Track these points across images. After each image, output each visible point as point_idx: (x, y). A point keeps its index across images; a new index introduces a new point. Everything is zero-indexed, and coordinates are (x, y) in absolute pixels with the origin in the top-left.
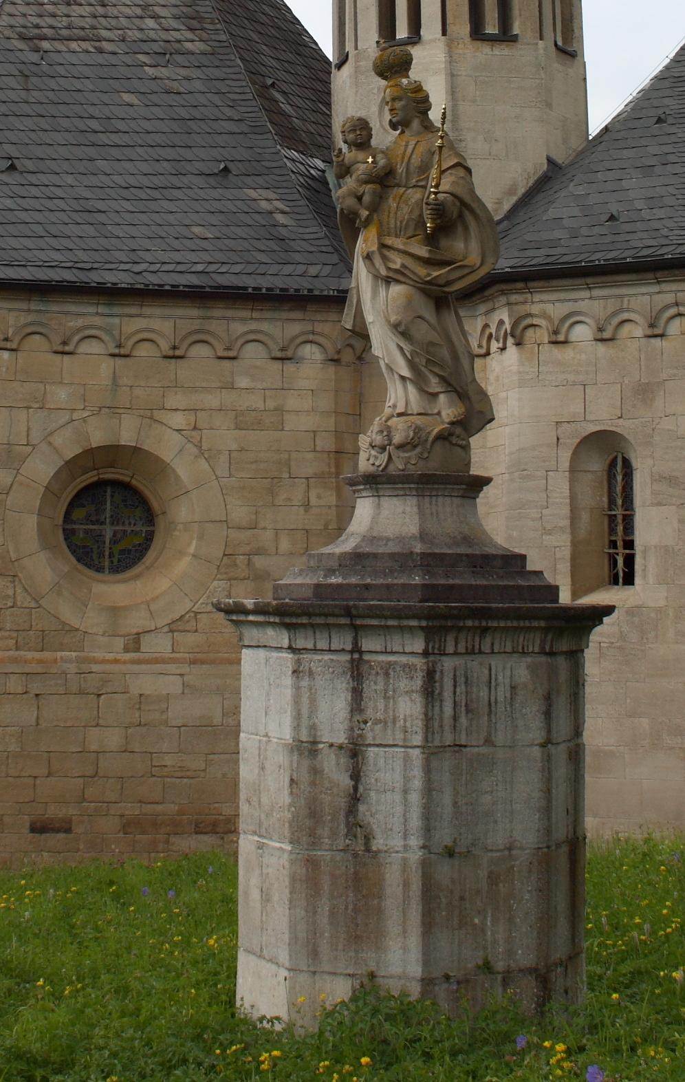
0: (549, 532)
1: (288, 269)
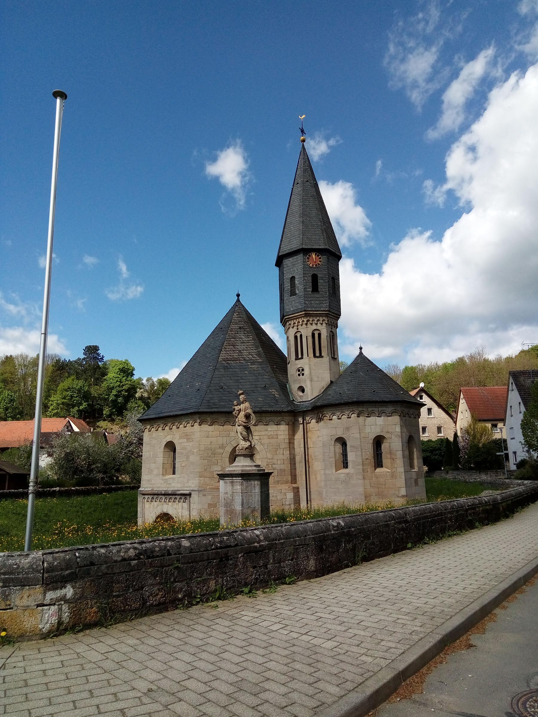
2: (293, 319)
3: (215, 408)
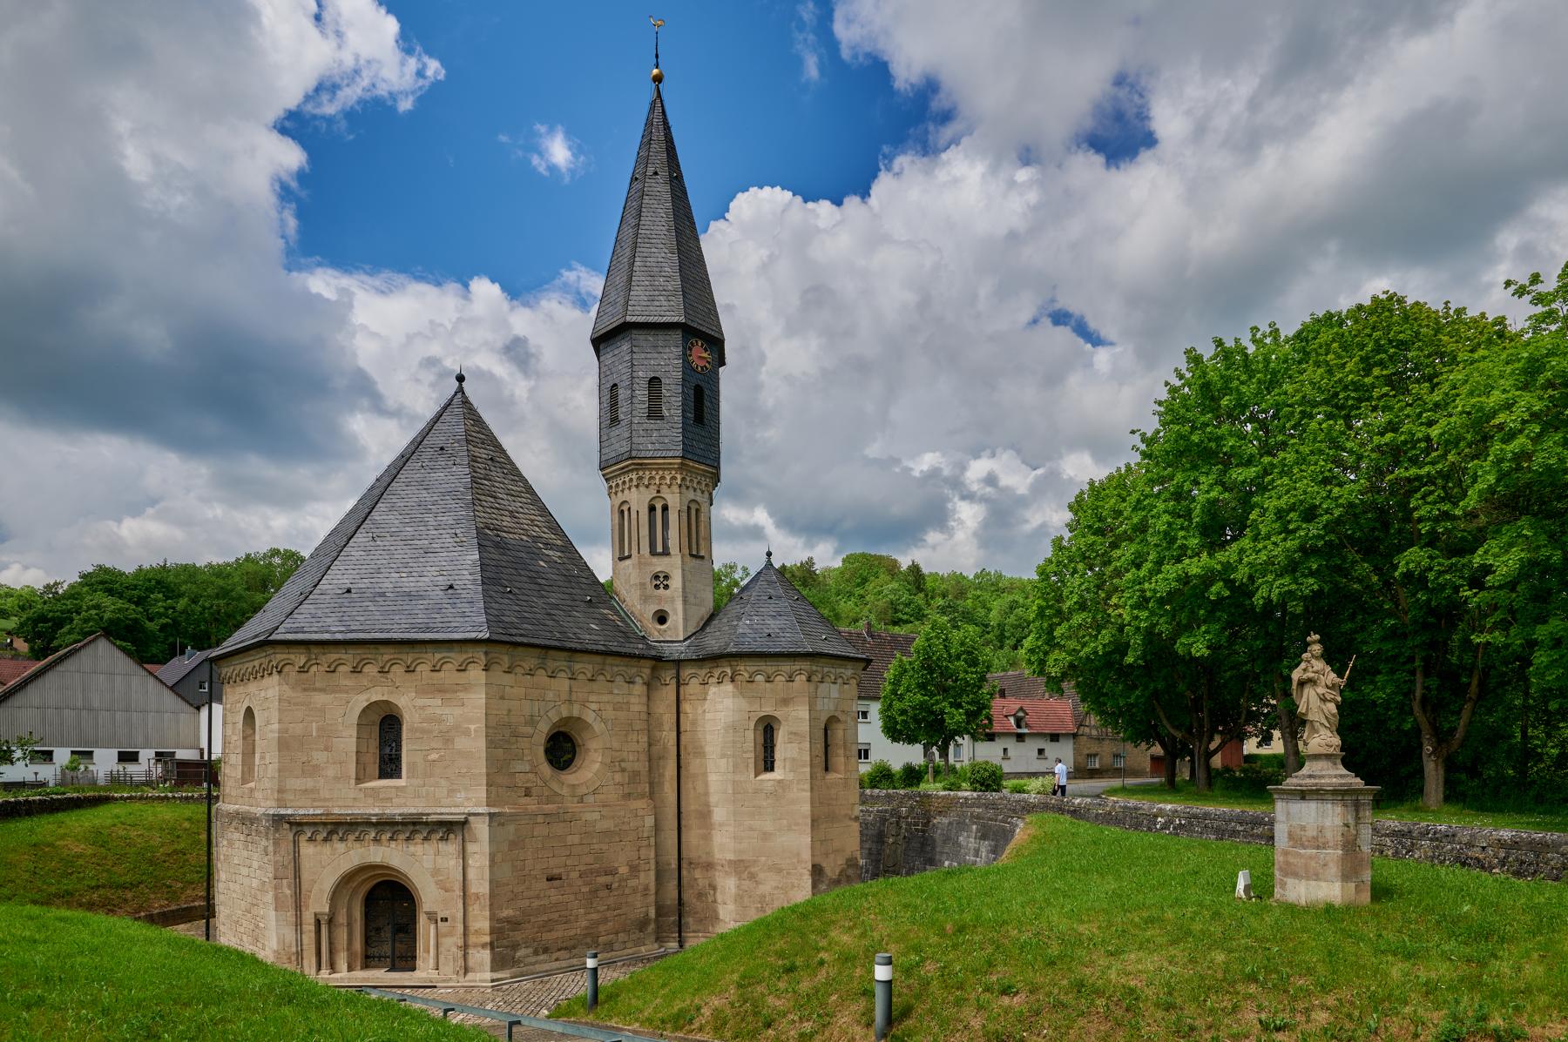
0: (745, 752)
1: (632, 645)
2: (651, 469)
3: (521, 635)
